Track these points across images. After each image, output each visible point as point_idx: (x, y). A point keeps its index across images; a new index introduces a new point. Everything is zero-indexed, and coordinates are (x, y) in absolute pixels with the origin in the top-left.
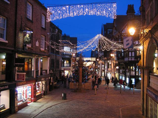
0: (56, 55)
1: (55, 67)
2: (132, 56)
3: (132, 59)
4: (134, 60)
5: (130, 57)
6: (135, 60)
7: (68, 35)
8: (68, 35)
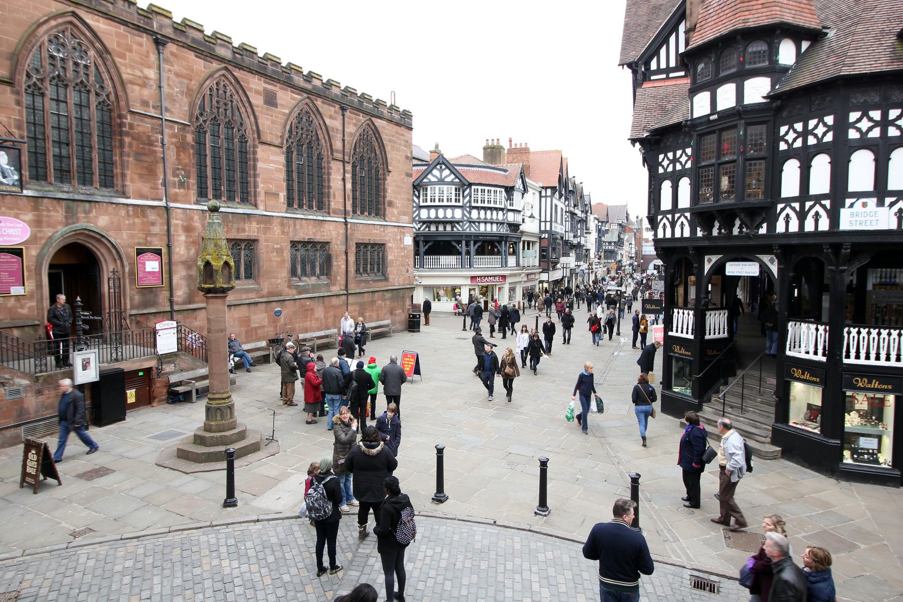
0: (346, 223)
1: (341, 279)
2: (675, 208)
3: (673, 224)
4: (687, 234)
5: (665, 213)
6: (693, 231)
7: (521, 144)
8: (521, 144)
